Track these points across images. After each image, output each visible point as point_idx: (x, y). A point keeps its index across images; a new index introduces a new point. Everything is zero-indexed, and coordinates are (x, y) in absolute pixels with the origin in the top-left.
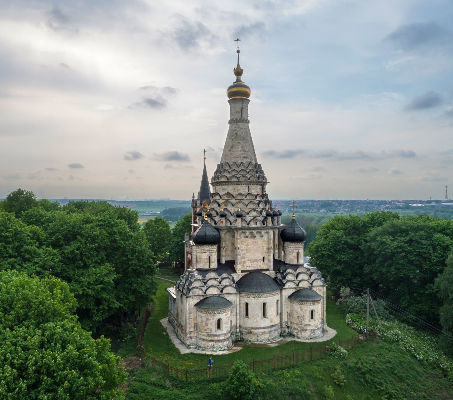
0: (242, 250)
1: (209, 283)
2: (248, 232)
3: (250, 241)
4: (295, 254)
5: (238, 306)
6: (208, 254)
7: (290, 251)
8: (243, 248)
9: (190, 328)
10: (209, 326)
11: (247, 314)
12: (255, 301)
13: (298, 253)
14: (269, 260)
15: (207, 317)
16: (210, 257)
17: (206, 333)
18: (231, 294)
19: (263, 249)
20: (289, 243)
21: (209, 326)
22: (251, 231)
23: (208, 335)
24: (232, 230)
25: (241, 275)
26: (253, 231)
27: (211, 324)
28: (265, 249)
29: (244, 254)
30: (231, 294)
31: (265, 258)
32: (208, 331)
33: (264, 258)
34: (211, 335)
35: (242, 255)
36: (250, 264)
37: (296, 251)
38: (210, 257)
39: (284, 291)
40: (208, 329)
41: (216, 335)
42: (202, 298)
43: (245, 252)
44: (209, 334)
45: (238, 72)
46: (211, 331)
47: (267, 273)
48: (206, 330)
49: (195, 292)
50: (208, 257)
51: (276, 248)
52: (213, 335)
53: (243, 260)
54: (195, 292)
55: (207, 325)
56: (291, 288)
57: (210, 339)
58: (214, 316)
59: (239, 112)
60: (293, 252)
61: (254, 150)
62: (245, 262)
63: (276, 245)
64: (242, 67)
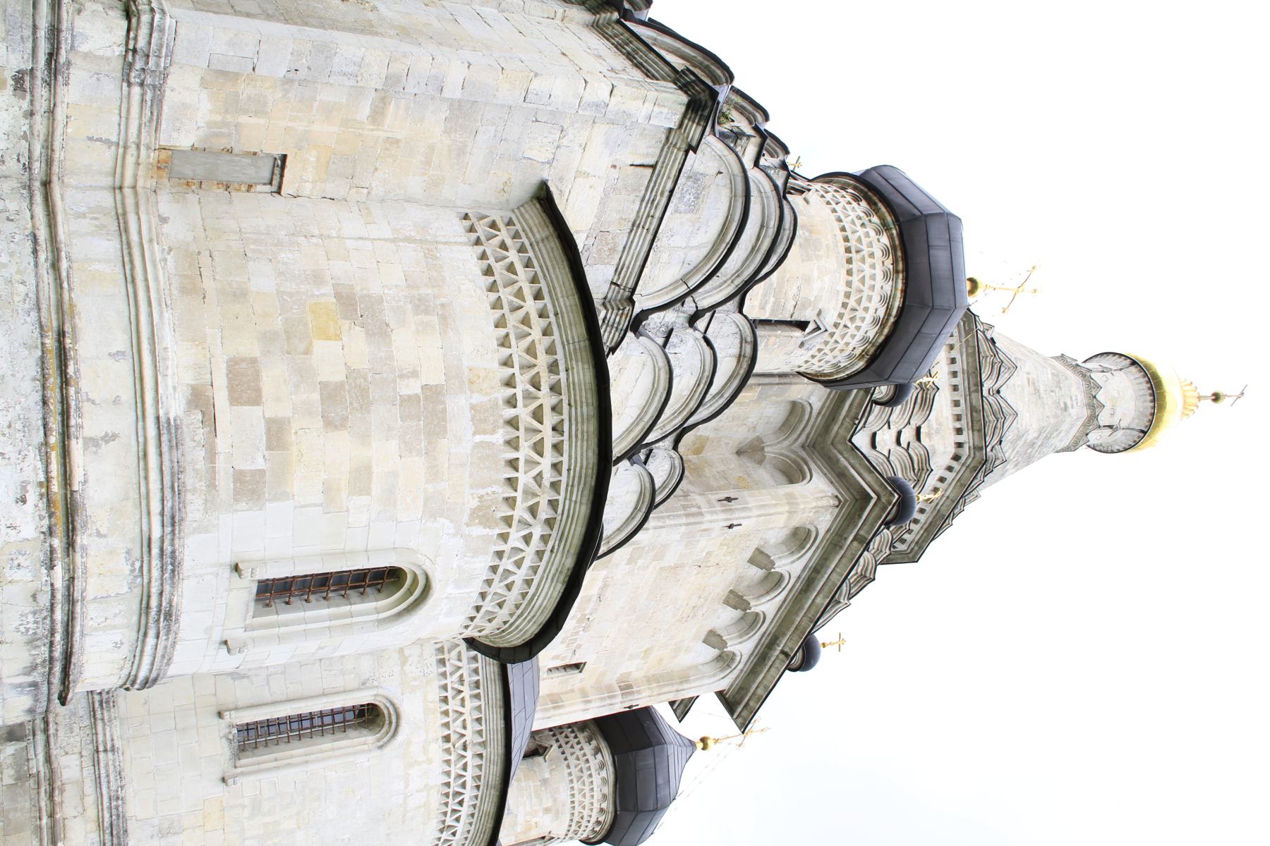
7: (564, 796)
9: (219, 76)
10: (321, 453)
11: (256, 737)
15: (459, 407)
16: (802, 325)
17: (199, 399)
21: (321, 453)
23: (168, 431)
27: (361, 479)
31: (575, 675)
32: (239, 433)
33: (578, 666)
34: (175, 488)
38: (802, 325)
40: (276, 434)
41: (161, 557)
43: (670, 559)
44: (194, 456)
46: (249, 487)
48: (245, 387)
49: (693, 208)
50: (807, 315)
52: (173, 521)
54: (693, 208)
55: (342, 403)
57: (103, 479)
58: (481, 515)
60: (557, 814)
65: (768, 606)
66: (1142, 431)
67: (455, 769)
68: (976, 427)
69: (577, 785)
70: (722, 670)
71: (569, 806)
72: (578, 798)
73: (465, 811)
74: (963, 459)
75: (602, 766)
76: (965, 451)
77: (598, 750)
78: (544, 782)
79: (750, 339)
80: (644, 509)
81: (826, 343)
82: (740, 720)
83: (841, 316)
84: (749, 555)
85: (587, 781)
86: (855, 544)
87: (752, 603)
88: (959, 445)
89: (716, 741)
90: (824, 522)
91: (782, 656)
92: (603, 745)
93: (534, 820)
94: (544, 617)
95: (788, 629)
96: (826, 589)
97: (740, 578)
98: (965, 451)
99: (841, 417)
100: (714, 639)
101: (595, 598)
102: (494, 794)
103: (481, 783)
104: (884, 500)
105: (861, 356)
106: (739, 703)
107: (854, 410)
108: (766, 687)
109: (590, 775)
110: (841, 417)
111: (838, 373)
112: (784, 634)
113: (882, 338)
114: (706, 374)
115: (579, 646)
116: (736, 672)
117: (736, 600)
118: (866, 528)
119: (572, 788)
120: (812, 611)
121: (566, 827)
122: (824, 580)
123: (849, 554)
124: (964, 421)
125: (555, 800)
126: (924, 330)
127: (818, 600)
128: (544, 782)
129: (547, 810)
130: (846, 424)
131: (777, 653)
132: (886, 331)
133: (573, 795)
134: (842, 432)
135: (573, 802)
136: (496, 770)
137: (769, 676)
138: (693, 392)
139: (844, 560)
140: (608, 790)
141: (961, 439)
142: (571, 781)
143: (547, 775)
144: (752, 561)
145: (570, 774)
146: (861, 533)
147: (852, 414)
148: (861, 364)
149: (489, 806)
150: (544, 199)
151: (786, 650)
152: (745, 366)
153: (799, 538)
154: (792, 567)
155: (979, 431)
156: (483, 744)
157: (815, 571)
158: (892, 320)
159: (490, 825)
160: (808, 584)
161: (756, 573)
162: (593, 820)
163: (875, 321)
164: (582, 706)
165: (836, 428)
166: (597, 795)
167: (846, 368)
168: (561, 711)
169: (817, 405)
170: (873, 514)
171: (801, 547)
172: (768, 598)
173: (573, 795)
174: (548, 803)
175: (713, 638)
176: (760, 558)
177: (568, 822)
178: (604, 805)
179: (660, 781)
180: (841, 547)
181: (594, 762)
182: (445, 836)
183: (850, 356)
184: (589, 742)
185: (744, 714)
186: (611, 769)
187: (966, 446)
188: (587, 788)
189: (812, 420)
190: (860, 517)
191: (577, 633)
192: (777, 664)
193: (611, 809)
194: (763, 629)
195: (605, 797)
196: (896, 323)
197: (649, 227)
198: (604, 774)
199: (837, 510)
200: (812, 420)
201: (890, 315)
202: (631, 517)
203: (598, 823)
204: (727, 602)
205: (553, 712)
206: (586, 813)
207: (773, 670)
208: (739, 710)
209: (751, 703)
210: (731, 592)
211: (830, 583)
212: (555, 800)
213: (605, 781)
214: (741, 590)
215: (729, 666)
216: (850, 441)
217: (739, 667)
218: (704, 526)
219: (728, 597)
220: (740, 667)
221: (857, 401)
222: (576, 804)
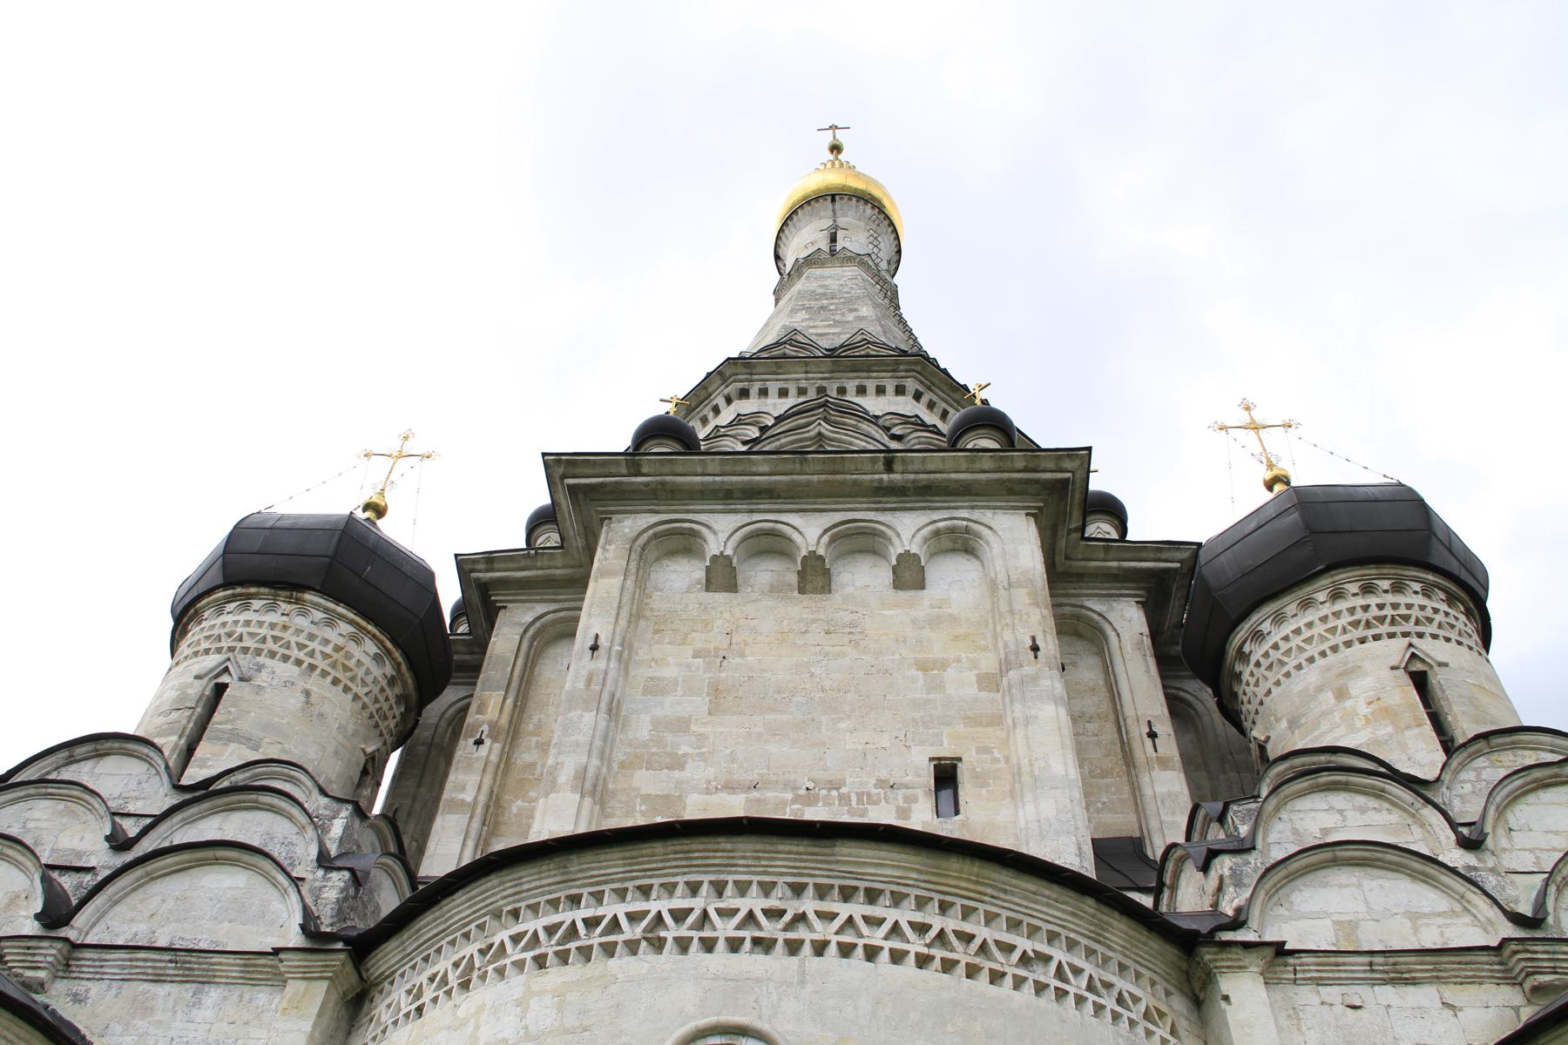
0: (656, 688)
3: (764, 611)
6: (213, 660)
7: (1311, 676)
8: (668, 672)
12: (542, 1013)
13: (1421, 681)
16: (220, 689)
19: (939, 686)
20: (1261, 619)
22: (764, 518)
26: (794, 519)
28: (961, 685)
29: (682, 725)
35: (641, 728)
39: (1244, 994)
43: (696, 705)
51: (1143, 749)
63: (1138, 732)
65: (809, 530)
66: (833, 200)
67: (513, 953)
68: (703, 393)
69: (1292, 663)
70: (978, 536)
71: (1331, 657)
72: (1312, 650)
73: (612, 908)
74: (741, 385)
75: (1258, 636)
76: (732, 389)
77: (1243, 657)
78: (1293, 724)
79: (64, 754)
80: (254, 797)
81: (245, 650)
82: (1067, 464)
83: (219, 650)
84: (720, 597)
85: (1284, 646)
86: (645, 470)
87: (804, 553)
88: (729, 401)
89: (1270, 466)
91: (897, 466)
92: (1231, 651)
93: (1363, 709)
94: (492, 881)
95: (843, 483)
96: (738, 469)
97: (775, 589)
98: (732, 389)
99: (540, 572)
100: (907, 576)
101: (756, 794)
102: (578, 864)
103: (562, 894)
104: (561, 470)
105: (298, 601)
106: (1037, 481)
107: (523, 563)
108: (972, 460)
109: (1276, 647)
110: (540, 572)
111: (342, 617)
112: (855, 482)
113: (263, 590)
114: (32, 791)
115: (881, 783)
116: (976, 514)
117: (814, 576)
118: (613, 470)
119: (1299, 667)
120: (789, 467)
121: (1385, 642)
122: (726, 478)
123: (666, 469)
124: (705, 412)
125: (1320, 689)
126: (256, 547)
127: (765, 468)
128: (1293, 724)
129: (1341, 694)
130: (546, 563)
131: (893, 476)
132: (253, 590)
133: (1311, 660)
134: (559, 563)
135: (1323, 654)
136: (531, 878)
137: (949, 465)
138: (62, 798)
139: (679, 469)
140: (1289, 604)
141: (721, 401)
142: (1288, 675)
143: (1284, 724)
144: (732, 587)
145: (1278, 683)
146: (624, 471)
147: (529, 562)
148: (308, 596)
149: (613, 863)
151: (880, 466)
152: (108, 745)
153: (683, 543)
154: (722, 531)
155: (706, 388)
156: (497, 915)
157: (727, 497)
158: (239, 590)
159: (658, 847)
160: (751, 495)
161: (763, 573)
162: (1360, 601)
163: (246, 607)
164: (1020, 733)
165: (558, 572)
166: (1312, 615)
167: (326, 610)
168: (1025, 762)
169: (540, 609)
170: (589, 471)
171: (694, 534)
172: (795, 536)
173: (1311, 660)
174: (1328, 697)
175: (909, 575)
176: (722, 577)
177: (1371, 644)
178: (1321, 596)
179: (1253, 525)
180: (663, 484)
181: (1257, 651)
182: (671, 931)
183: (303, 614)
184: (1238, 676)
185: (1052, 465)
186: (1255, 618)
187: (726, 391)
188: (1296, 641)
189: (566, 605)
190: (602, 484)
191: (841, 797)
192: (917, 466)
193: (1325, 581)
194: (871, 515)
195: (1306, 604)
196: (242, 584)
198: (1266, 627)
199: (615, 517)
200: (566, 605)
201: (234, 595)
202: (271, 809)
203: (1368, 589)
204: (826, 588)
205: (1026, 778)
206: (1346, 619)
207: (931, 467)
208: (1048, 476)
209: (1020, 464)
210: (802, 591)
211: (728, 468)
212: (1320, 689)
213: (1279, 619)
214: (793, 578)
215: (967, 530)
216: (561, 547)
217: (962, 514)
218: (581, 685)
219: (815, 591)
220: (964, 514)
221: (510, 565)
222: (1325, 646)
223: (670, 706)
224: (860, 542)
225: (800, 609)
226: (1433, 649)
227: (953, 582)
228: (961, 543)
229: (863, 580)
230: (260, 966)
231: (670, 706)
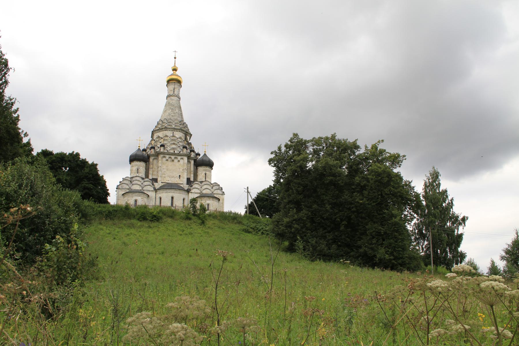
1: (134, 183)
2: (167, 156)
3: (170, 163)
4: (203, 174)
5: (154, 200)
14: (183, 178)
18: (149, 191)
24: (157, 154)
25: (161, 185)
28: (181, 170)
30: (149, 191)
36: (169, 179)
37: (204, 172)
39: (190, 194)
42: (128, 191)
43: (166, 170)
45: (175, 70)
47: (182, 185)
53: (164, 176)
56: (196, 193)
59: (171, 91)
61: (182, 114)
62: (165, 177)
64: (177, 65)
65: (173, 157)
90: (162, 156)
117: (173, 161)
150: (123, 195)
153: (165, 157)
161: (170, 160)
175: (179, 161)
176: (167, 160)
197: (124, 189)
217: (182, 157)
223: (165, 170)
224: (176, 158)
225: (172, 163)
226: (207, 172)
227: (181, 161)
228: (182, 159)
229: (176, 161)
230: (152, 191)
231: (165, 170)
